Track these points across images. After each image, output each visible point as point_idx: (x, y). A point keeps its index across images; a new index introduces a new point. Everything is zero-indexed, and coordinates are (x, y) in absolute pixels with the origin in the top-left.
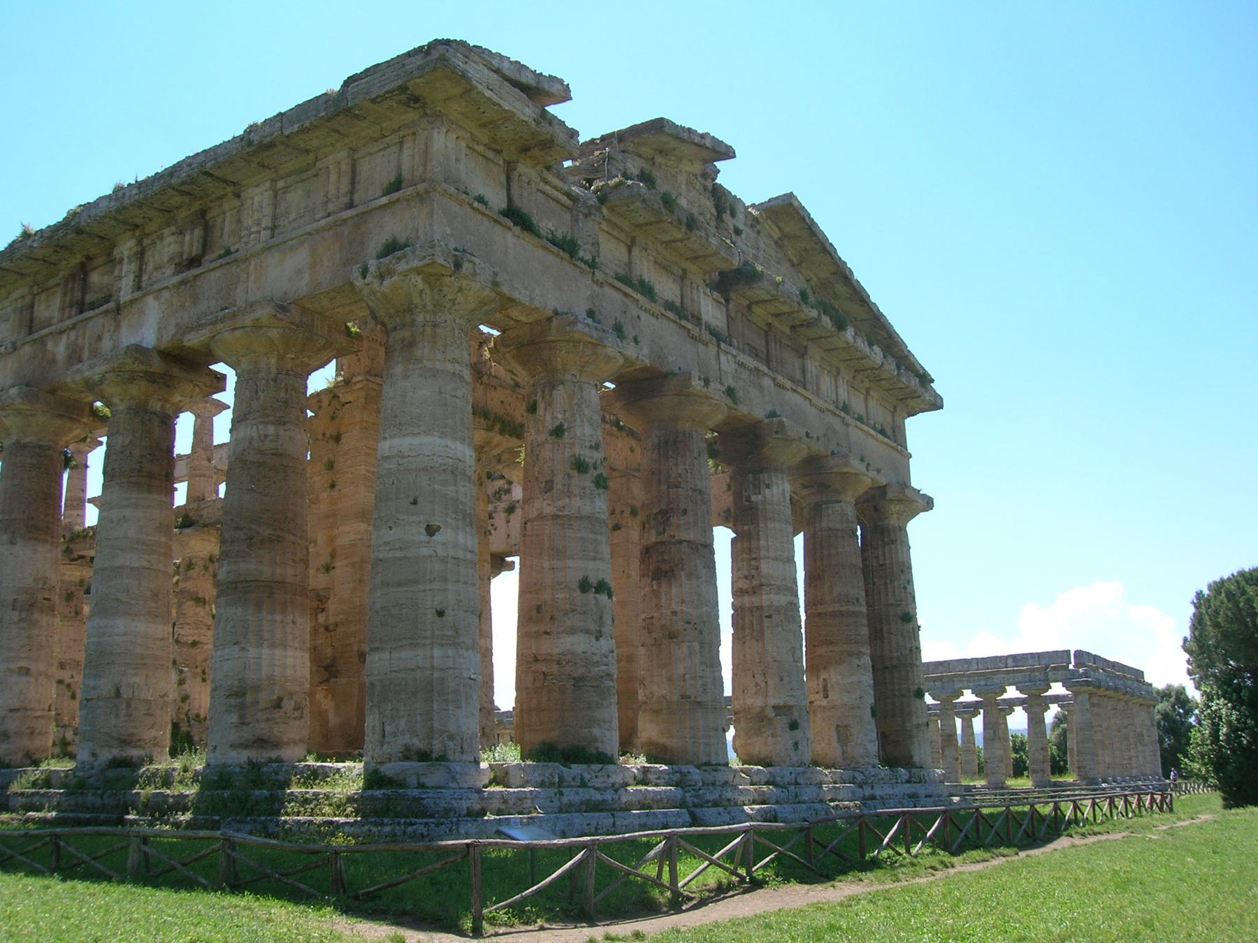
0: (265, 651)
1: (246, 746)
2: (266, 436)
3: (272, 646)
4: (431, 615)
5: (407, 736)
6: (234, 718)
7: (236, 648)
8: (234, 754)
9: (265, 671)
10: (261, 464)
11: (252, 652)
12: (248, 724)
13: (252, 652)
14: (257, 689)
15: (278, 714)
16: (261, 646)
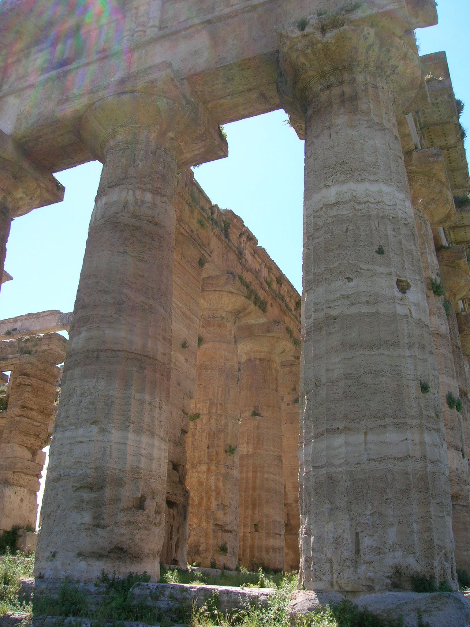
0: (131, 436)
1: (99, 556)
2: (143, 202)
3: (139, 431)
4: (414, 389)
5: (399, 554)
6: (87, 518)
7: (95, 429)
8: (83, 565)
9: (130, 460)
10: (137, 228)
11: (115, 435)
12: (104, 527)
13: (115, 435)
14: (119, 482)
15: (141, 517)
16: (126, 428)
